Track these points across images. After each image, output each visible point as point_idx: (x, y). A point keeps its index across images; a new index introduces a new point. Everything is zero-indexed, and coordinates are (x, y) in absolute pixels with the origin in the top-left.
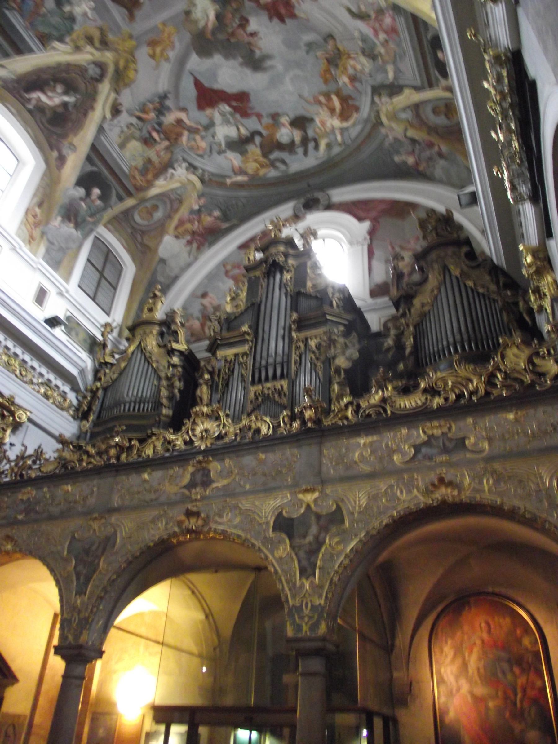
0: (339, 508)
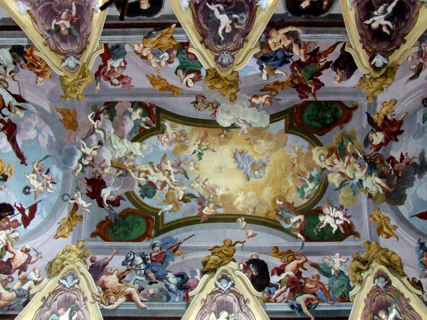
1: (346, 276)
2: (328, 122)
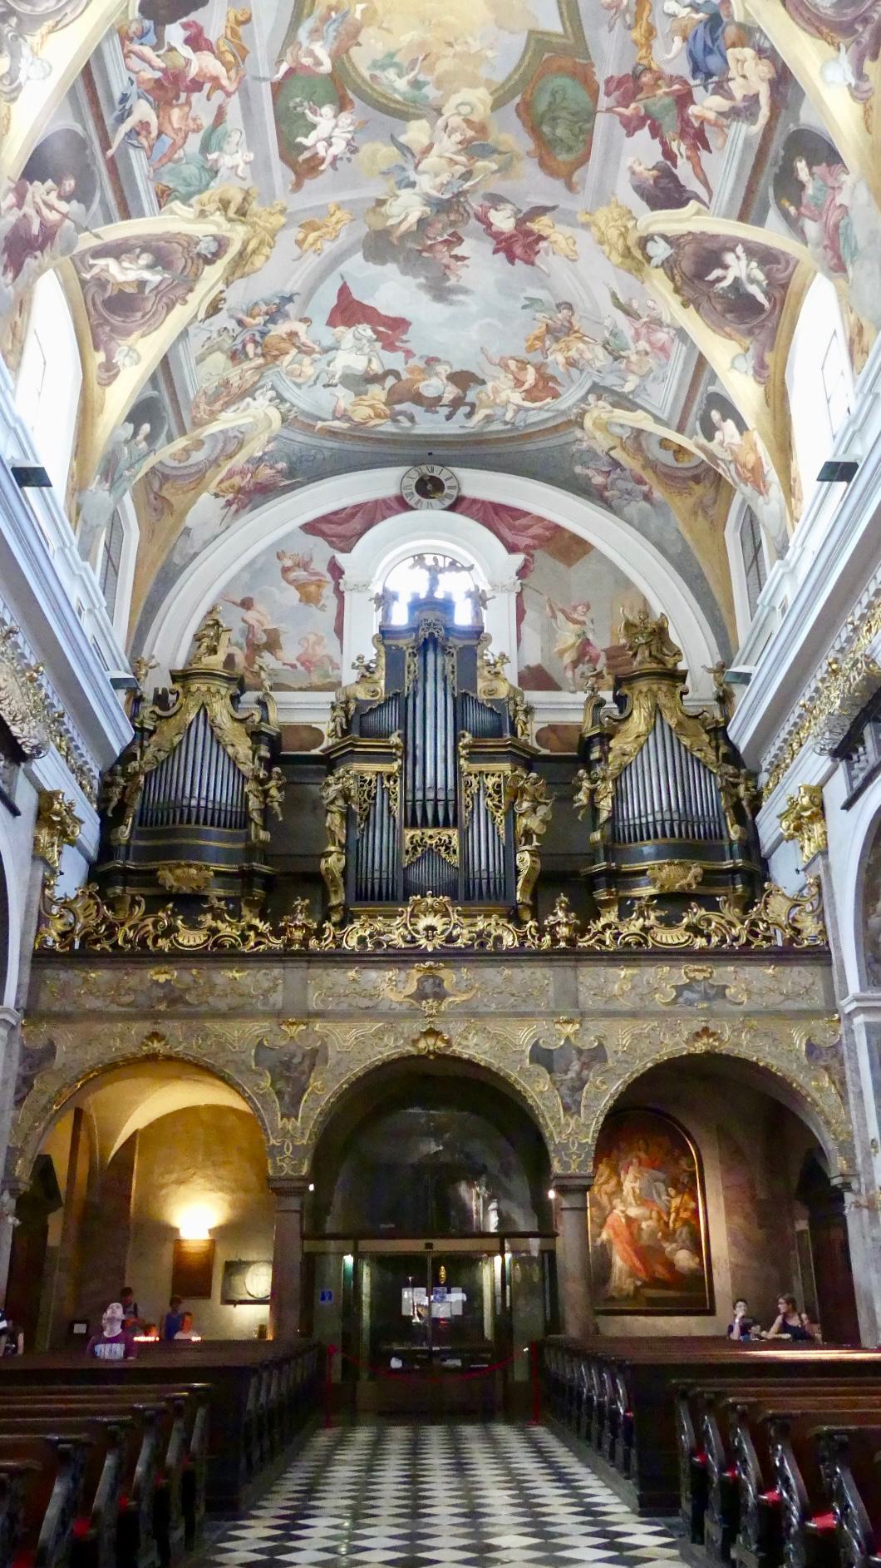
0: (601, 1045)
1: (208, 184)
2: (546, 129)
